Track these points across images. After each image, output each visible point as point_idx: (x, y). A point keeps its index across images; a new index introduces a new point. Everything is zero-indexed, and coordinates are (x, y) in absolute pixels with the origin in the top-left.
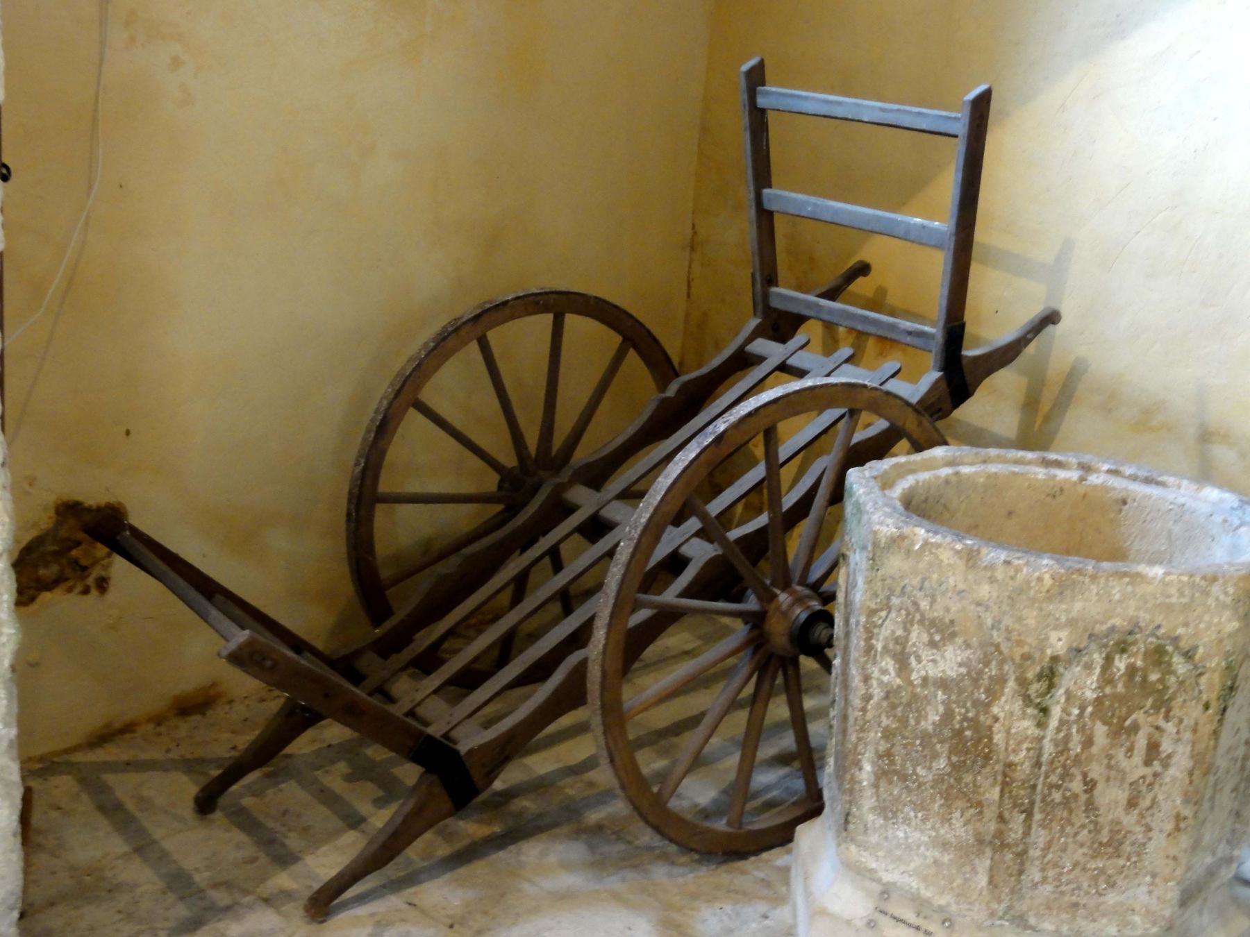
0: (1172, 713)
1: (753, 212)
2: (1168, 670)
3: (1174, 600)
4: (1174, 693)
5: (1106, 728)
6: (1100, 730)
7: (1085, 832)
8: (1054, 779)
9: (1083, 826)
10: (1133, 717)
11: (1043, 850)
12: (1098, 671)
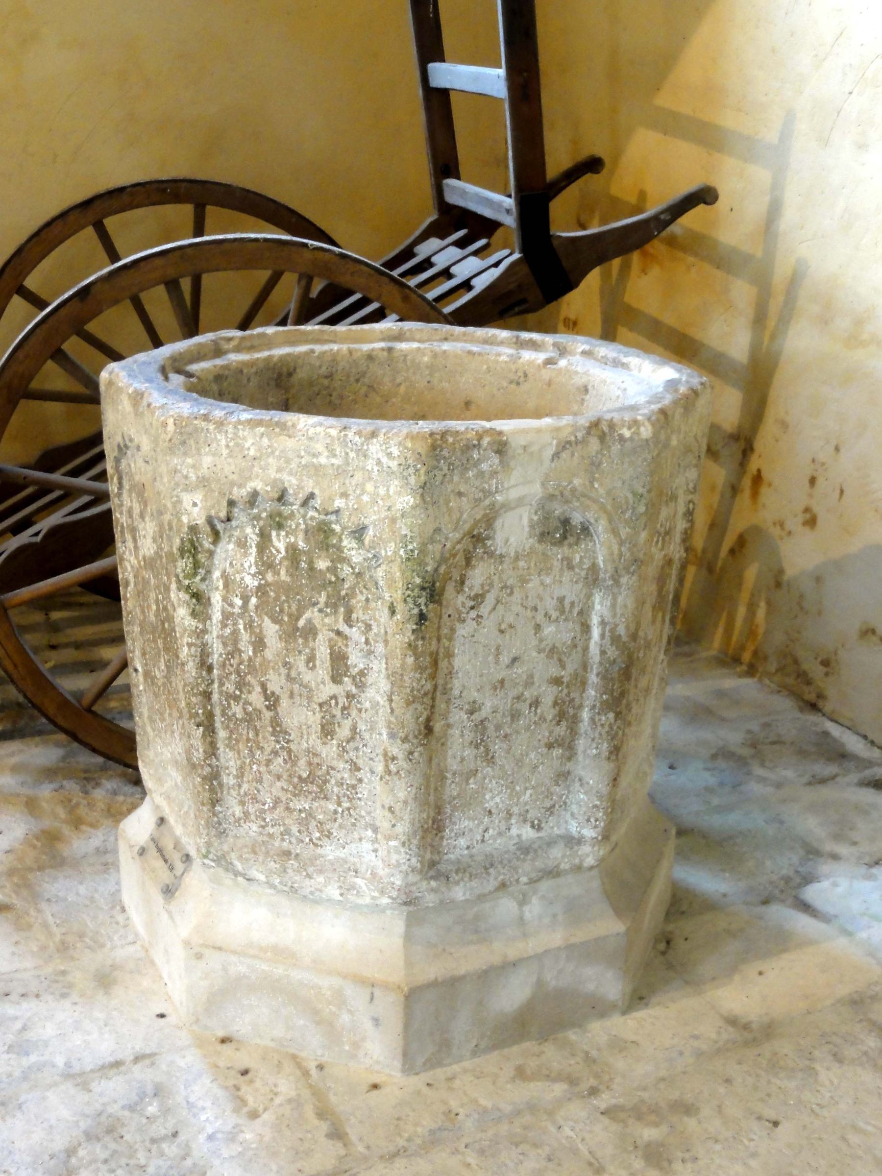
0: (354, 616)
1: (420, 92)
2: (339, 558)
3: (323, 460)
4: (352, 588)
5: (277, 627)
6: (271, 629)
7: (280, 760)
8: (230, 687)
9: (275, 753)
10: (307, 615)
11: (236, 777)
12: (254, 550)
